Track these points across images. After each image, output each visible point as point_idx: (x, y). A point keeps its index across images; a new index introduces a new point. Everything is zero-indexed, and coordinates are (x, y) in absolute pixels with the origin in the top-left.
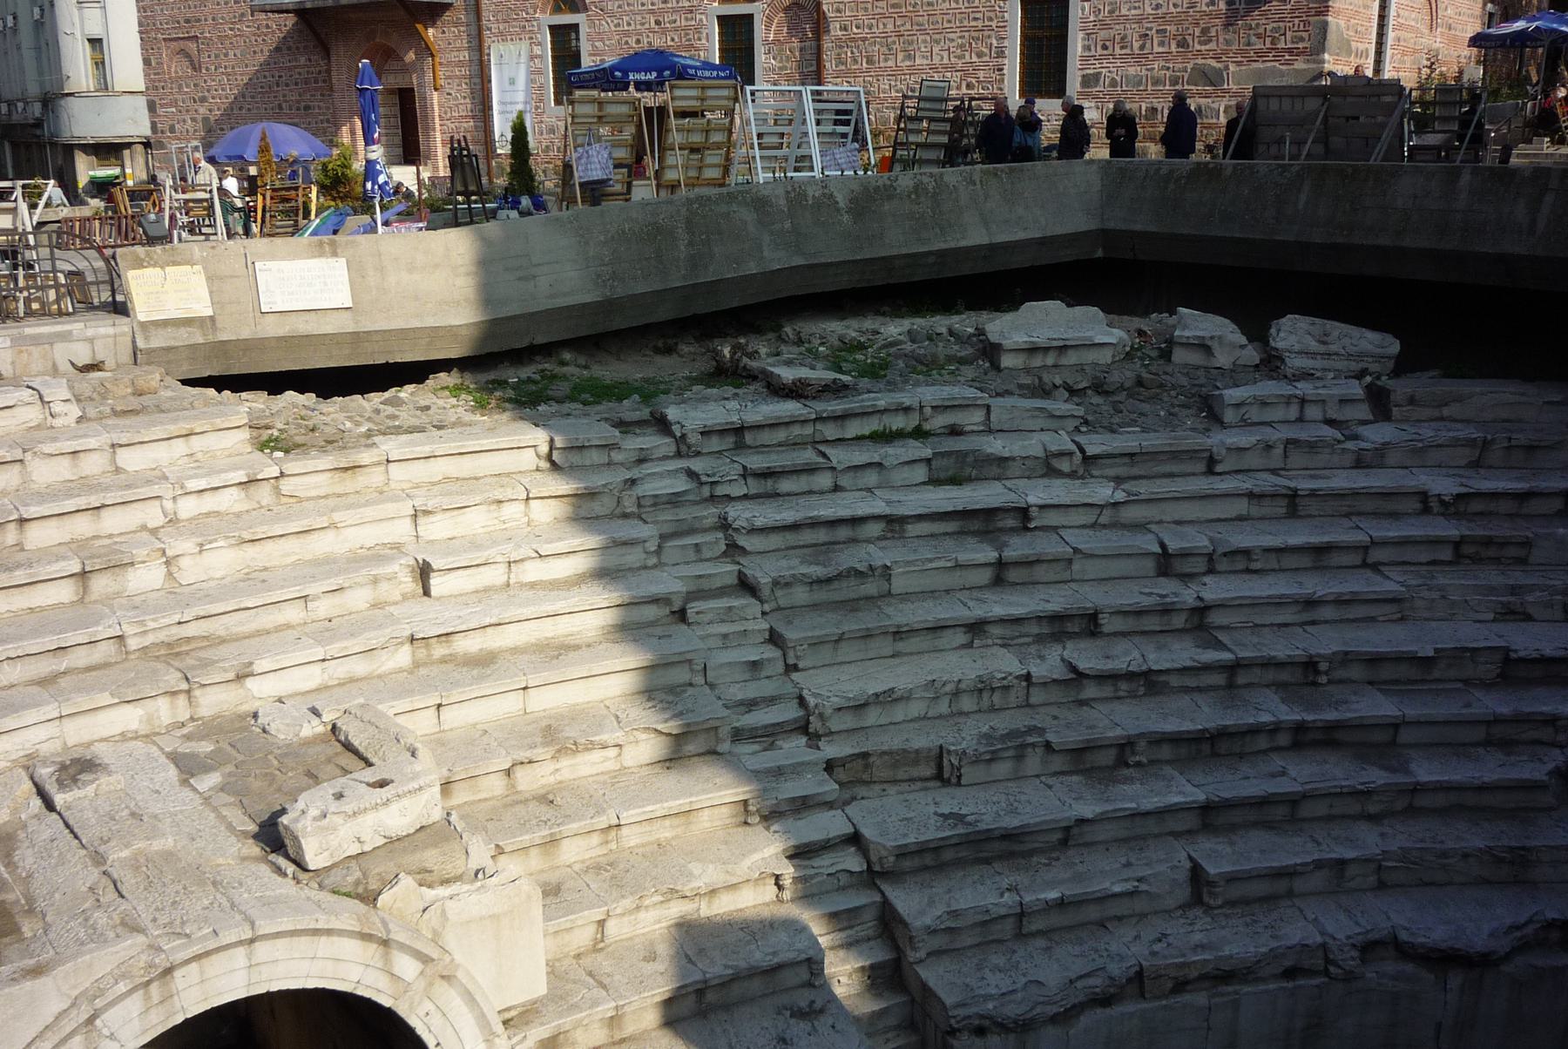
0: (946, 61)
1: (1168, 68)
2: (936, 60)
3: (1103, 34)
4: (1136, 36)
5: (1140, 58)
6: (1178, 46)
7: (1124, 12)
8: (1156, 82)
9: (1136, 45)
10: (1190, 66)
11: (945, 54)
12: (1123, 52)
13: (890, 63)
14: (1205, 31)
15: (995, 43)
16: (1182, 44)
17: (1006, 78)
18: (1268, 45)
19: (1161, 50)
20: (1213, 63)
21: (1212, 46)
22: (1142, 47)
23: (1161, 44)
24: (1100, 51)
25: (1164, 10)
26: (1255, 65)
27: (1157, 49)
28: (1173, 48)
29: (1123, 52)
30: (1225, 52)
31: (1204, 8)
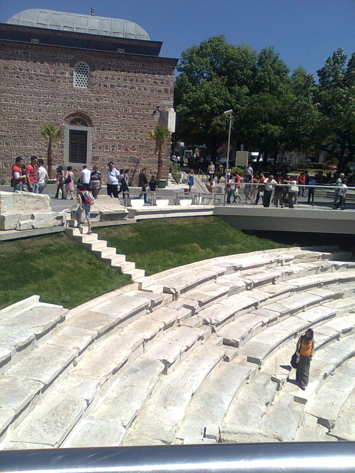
0: (40, 147)
1: (122, 157)
2: (36, 147)
3: (99, 144)
4: (111, 146)
5: (113, 152)
6: (125, 150)
7: (106, 138)
8: (118, 161)
9: (111, 149)
10: (129, 157)
11: (40, 145)
12: (107, 150)
13: (17, 146)
14: (133, 147)
15: (60, 143)
16: (126, 150)
17: (64, 155)
18: (153, 153)
19: (119, 151)
20: (136, 157)
21: (136, 151)
22: (113, 150)
23: (119, 149)
24: (98, 149)
25: (120, 139)
26: (149, 158)
27: (118, 151)
28: (123, 151)
29: (107, 150)
30: (140, 154)
31: (133, 140)
